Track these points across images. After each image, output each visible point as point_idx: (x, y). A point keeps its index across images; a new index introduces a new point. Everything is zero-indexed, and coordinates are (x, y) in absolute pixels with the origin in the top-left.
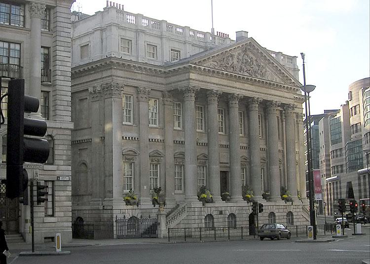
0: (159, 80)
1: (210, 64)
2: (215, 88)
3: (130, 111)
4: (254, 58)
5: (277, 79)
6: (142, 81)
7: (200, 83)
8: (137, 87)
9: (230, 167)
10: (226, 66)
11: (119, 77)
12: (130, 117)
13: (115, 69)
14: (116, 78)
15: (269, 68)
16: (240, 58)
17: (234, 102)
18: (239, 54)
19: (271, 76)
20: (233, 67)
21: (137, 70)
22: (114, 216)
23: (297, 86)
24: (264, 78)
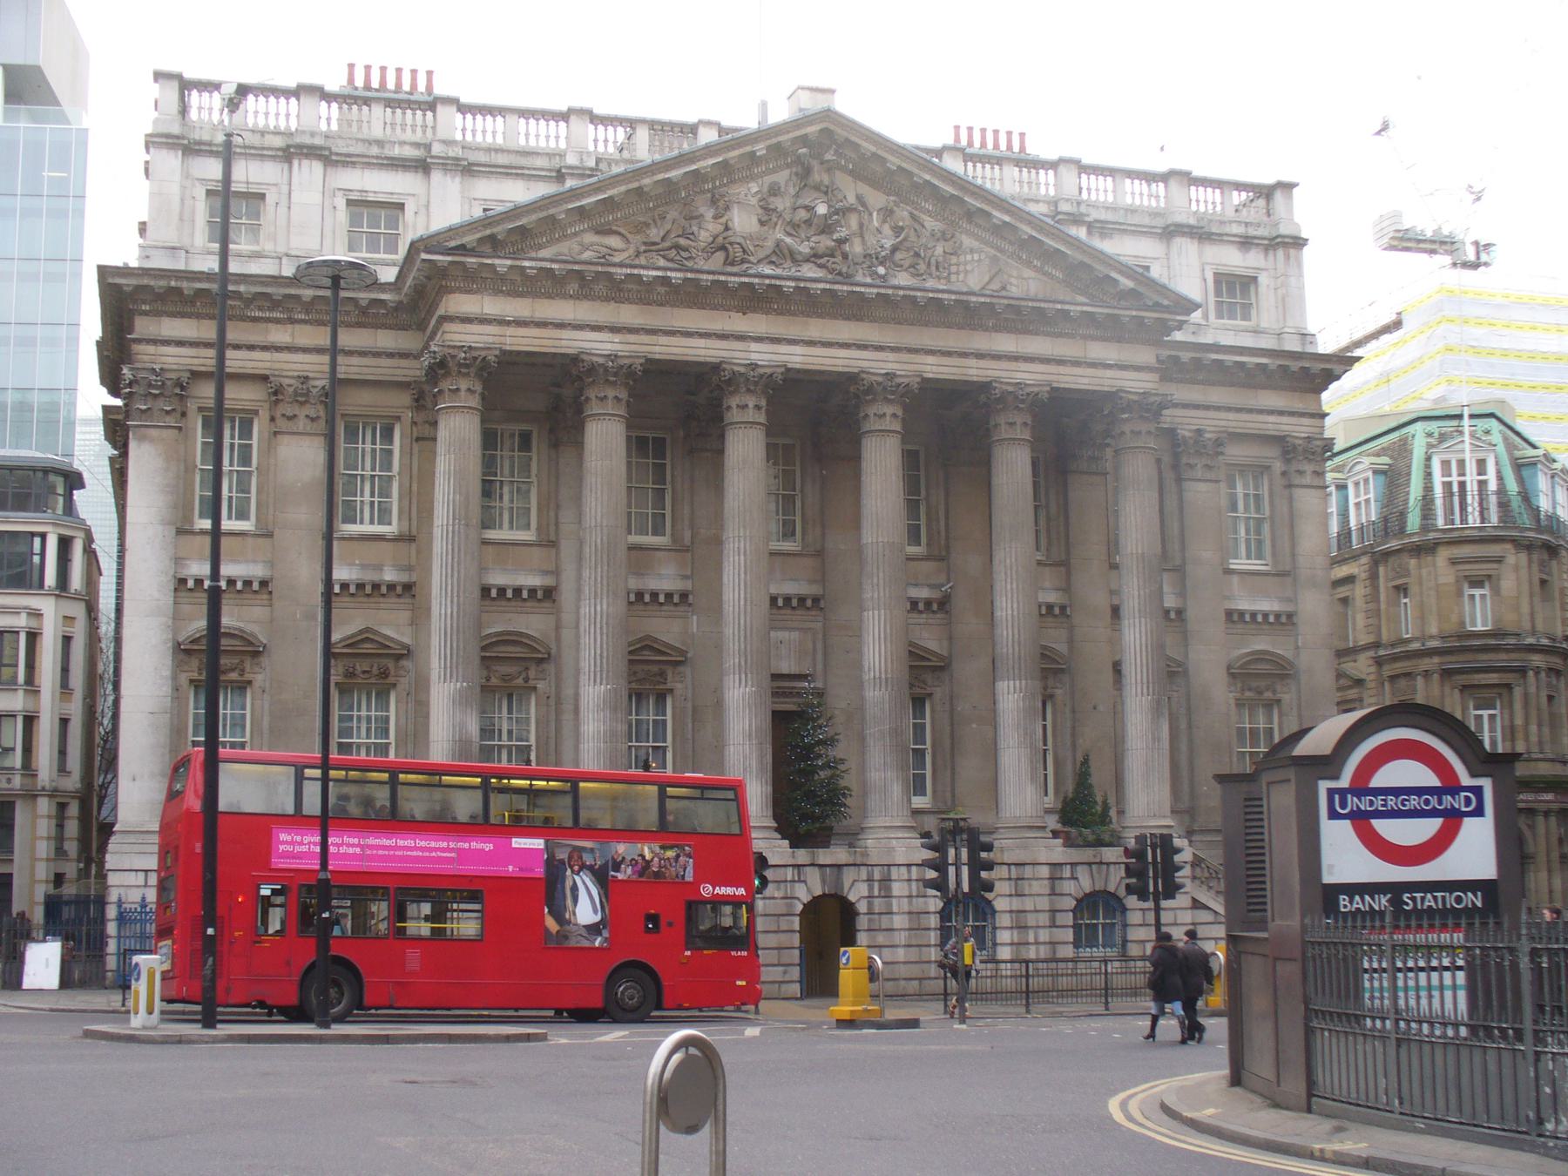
0: (386, 339)
1: (583, 247)
2: (600, 345)
3: (1259, 522)
4: (876, 199)
5: (1025, 283)
6: (294, 349)
7: (510, 331)
8: (265, 378)
9: (820, 694)
10: (677, 247)
11: (166, 342)
12: (1260, 542)
13: (146, 313)
14: (151, 349)
15: (978, 238)
16: (781, 204)
17: (734, 401)
18: (774, 191)
19: (972, 271)
20: (723, 248)
21: (260, 309)
22: (113, 896)
23: (1157, 306)
24: (930, 284)
